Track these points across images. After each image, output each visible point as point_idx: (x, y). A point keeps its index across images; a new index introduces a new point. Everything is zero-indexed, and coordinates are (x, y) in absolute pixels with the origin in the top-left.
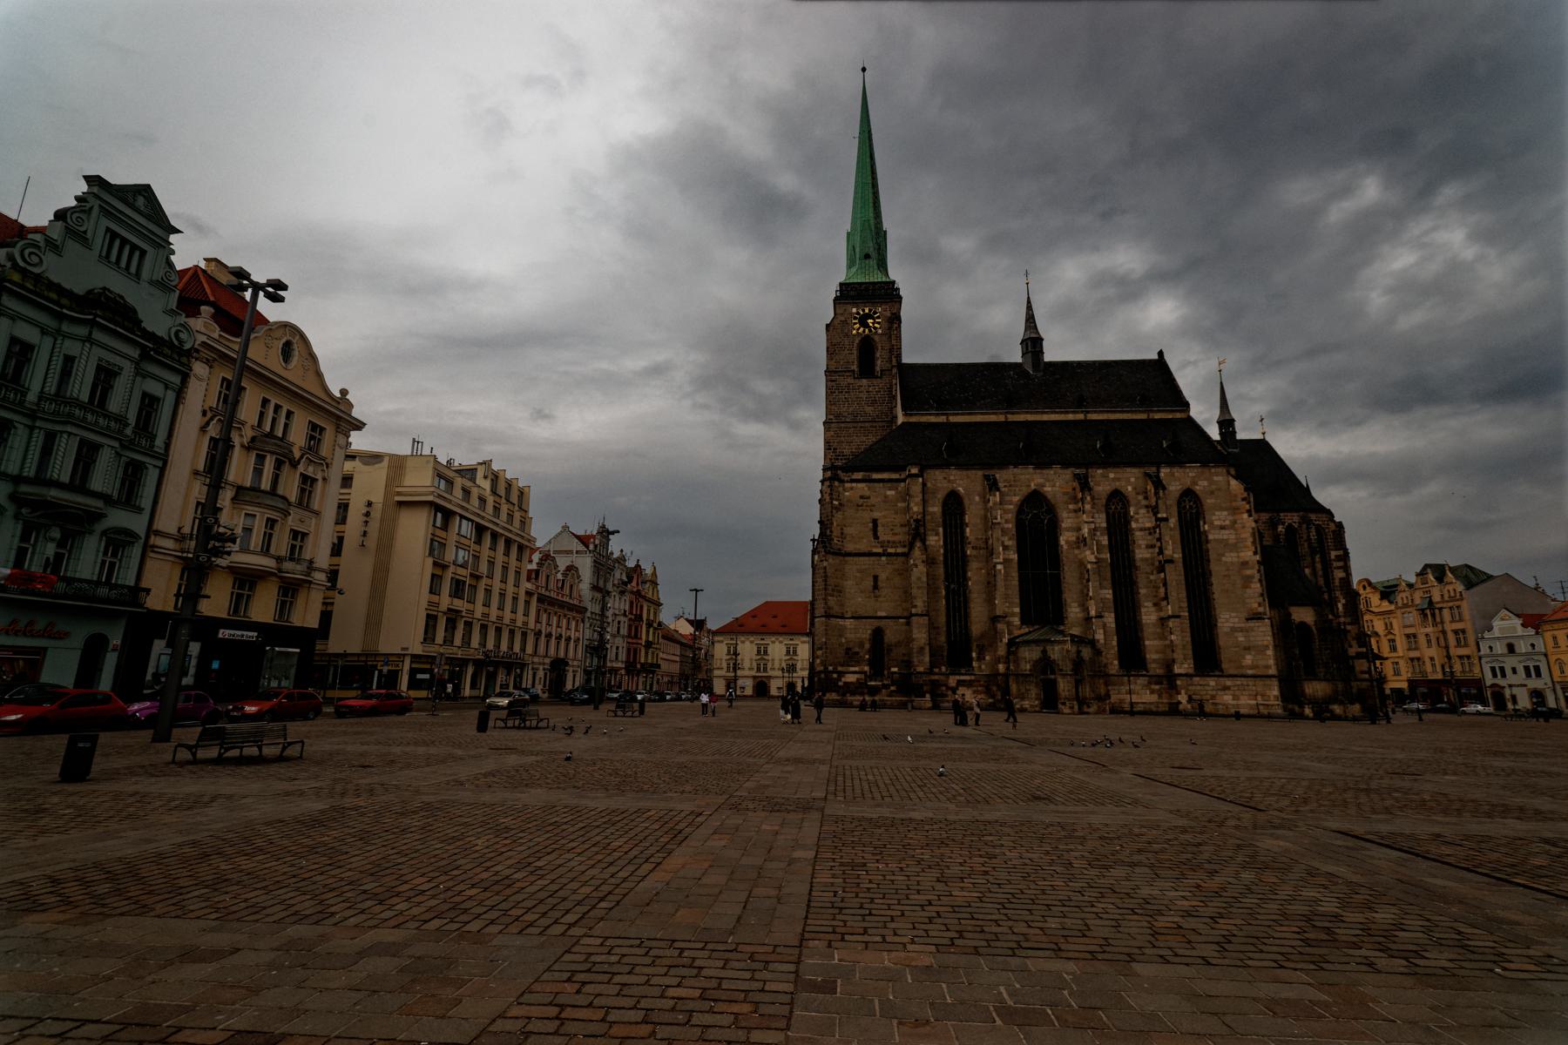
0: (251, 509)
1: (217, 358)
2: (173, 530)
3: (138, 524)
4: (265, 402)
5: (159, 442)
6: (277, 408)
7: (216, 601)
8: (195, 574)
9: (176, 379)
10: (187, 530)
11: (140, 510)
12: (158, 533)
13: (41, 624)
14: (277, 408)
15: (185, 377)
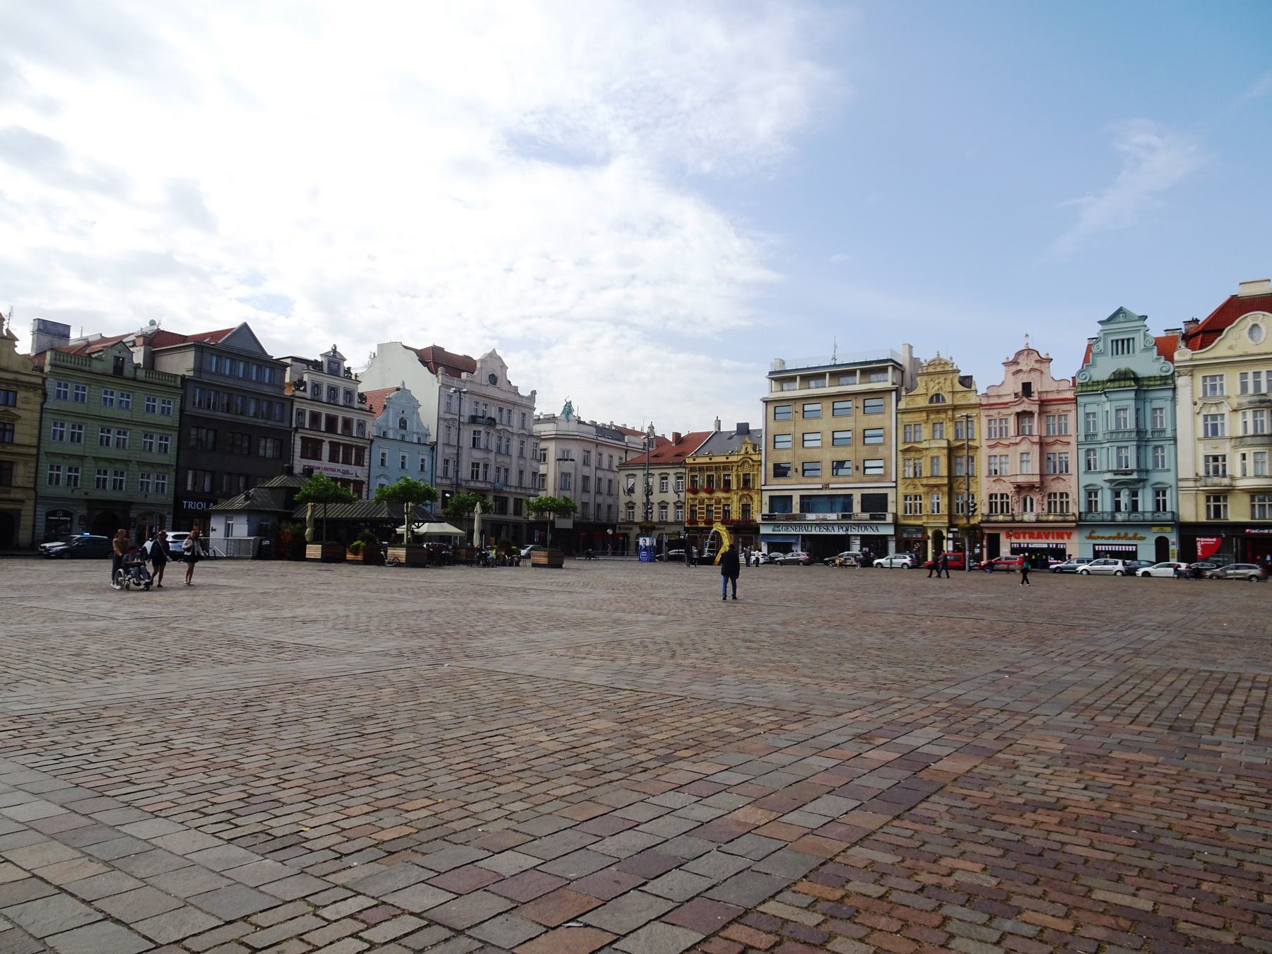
0: (1243, 450)
1: (1192, 369)
2: (1192, 476)
3: (1168, 478)
4: (1244, 375)
5: (1169, 434)
6: (1257, 374)
7: (1237, 512)
8: (1218, 497)
9: (1170, 393)
10: (1202, 473)
11: (1168, 470)
12: (1182, 480)
13: (1131, 535)
14: (1257, 374)
15: (1174, 389)
